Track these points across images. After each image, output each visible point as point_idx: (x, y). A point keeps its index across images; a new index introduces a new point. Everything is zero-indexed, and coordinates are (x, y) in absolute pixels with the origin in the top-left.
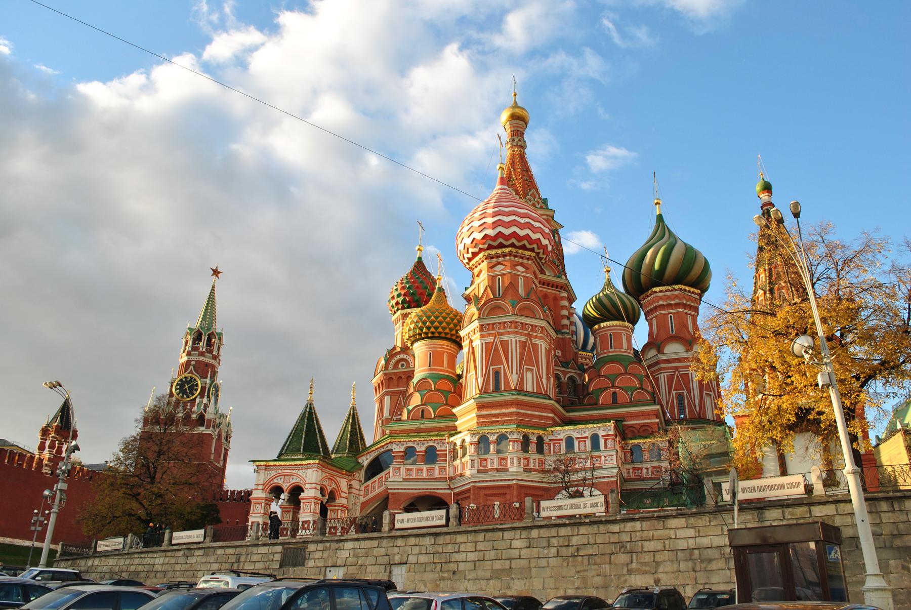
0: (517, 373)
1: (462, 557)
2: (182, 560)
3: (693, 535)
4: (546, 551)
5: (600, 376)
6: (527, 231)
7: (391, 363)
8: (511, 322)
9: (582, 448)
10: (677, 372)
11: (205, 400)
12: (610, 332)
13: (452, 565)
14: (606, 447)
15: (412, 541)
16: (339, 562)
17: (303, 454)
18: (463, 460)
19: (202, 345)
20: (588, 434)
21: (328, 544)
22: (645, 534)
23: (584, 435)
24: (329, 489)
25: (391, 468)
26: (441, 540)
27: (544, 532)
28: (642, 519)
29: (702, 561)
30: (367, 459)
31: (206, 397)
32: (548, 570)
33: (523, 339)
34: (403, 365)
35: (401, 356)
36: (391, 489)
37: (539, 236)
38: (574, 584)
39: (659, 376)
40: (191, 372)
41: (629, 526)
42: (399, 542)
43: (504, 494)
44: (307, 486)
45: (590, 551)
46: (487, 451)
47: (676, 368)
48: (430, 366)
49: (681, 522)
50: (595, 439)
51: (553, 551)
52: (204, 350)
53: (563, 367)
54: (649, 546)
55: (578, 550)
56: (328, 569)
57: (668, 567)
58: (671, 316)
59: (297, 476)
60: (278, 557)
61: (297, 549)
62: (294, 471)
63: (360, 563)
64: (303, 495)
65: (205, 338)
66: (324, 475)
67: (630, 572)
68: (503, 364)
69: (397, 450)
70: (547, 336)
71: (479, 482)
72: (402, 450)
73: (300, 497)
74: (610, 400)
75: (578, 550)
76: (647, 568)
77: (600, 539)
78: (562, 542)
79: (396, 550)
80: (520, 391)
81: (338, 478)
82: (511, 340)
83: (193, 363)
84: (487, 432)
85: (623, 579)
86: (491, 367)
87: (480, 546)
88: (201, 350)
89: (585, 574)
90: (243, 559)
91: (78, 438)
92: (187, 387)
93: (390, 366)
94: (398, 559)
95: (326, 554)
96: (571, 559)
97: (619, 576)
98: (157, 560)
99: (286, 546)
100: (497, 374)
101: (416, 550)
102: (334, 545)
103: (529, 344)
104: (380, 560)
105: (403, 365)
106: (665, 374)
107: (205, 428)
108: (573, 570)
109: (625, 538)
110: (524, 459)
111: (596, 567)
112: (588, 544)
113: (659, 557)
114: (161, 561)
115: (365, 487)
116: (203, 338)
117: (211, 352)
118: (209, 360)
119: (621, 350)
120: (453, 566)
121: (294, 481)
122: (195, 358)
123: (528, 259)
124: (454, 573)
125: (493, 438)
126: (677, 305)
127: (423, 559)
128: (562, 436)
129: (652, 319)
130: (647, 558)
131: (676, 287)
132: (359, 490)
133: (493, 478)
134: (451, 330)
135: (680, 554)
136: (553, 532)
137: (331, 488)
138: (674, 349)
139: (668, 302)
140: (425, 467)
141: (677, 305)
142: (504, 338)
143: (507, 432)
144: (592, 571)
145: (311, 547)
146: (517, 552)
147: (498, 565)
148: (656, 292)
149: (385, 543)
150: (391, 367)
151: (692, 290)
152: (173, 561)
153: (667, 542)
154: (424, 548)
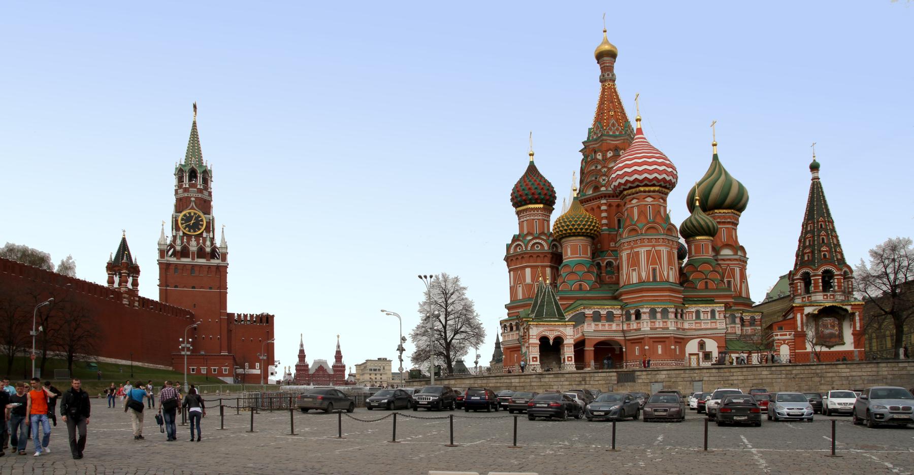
1: (736, 378)
2: (537, 380)
3: (849, 371)
4: (780, 376)
5: (698, 271)
6: (664, 176)
8: (663, 239)
9: (706, 317)
10: (728, 268)
12: (702, 243)
13: (730, 381)
14: (719, 317)
15: (705, 371)
16: (659, 380)
17: (558, 318)
20: (709, 310)
21: (650, 372)
22: (827, 370)
23: (707, 310)
25: (586, 323)
26: (722, 371)
27: (778, 368)
28: (826, 365)
29: (853, 381)
32: (782, 383)
35: (537, 241)
38: (794, 388)
40: (192, 208)
41: (820, 367)
42: (697, 371)
43: (664, 341)
44: (568, 337)
45: (802, 376)
46: (655, 317)
47: (728, 265)
48: (580, 255)
49: (844, 366)
50: (713, 312)
51: (784, 376)
54: (829, 375)
55: (796, 376)
56: (652, 384)
57: (838, 383)
59: (559, 331)
60: (615, 378)
61: (627, 374)
63: (673, 380)
67: (821, 384)
68: (658, 265)
69: (588, 313)
71: (650, 334)
72: (592, 313)
74: (703, 286)
75: (796, 376)
76: (829, 383)
77: (806, 372)
78: (788, 372)
79: (695, 375)
80: (667, 281)
85: (817, 387)
86: (651, 266)
87: (744, 373)
89: (799, 385)
90: (588, 379)
91: (140, 273)
92: (192, 222)
94: (697, 379)
95: (649, 377)
96: (793, 379)
97: (816, 386)
98: (513, 381)
99: (619, 373)
100: (654, 270)
101: (708, 375)
102: (656, 372)
104: (686, 379)
105: (537, 247)
108: (794, 384)
109: (818, 371)
111: (805, 382)
112: (801, 373)
113: (834, 379)
114: (517, 380)
120: (731, 382)
121: (556, 334)
124: (732, 384)
125: (658, 310)
126: (729, 223)
127: (712, 379)
128: (694, 310)
130: (828, 379)
131: (730, 211)
133: (660, 333)
135: (843, 378)
136: (783, 368)
138: (726, 252)
139: (723, 220)
140: (607, 324)
141: (729, 223)
142: (657, 248)
144: (803, 384)
145: (638, 373)
146: (765, 377)
147: (755, 381)
148: (717, 213)
149: (687, 371)
152: (529, 380)
153: (837, 374)
154: (712, 374)
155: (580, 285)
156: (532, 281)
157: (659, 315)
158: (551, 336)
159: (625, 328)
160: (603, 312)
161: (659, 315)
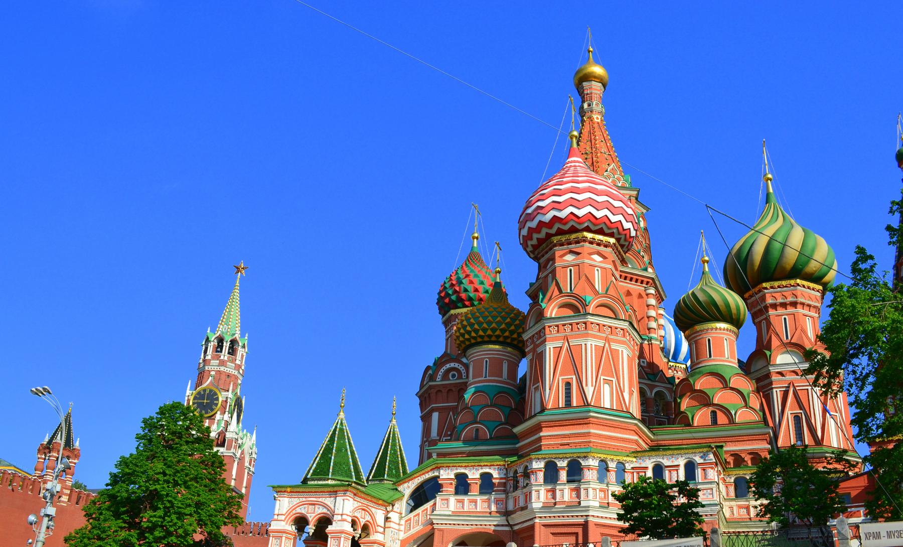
0: (592, 386)
7: (440, 373)
11: (226, 417)
18: (525, 490)
19: (224, 355)
24: (363, 522)
25: (438, 498)
30: (409, 487)
31: (227, 413)
33: (601, 343)
34: (454, 376)
36: (437, 524)
37: (620, 218)
39: (770, 392)
52: (226, 358)
53: (649, 379)
58: (785, 319)
59: (325, 506)
62: (320, 500)
64: (330, 528)
65: (226, 346)
66: (356, 504)
70: (629, 341)
73: (327, 530)
81: (373, 509)
82: (586, 344)
83: (213, 373)
84: (554, 456)
86: (561, 378)
88: (222, 358)
93: (439, 376)
100: (568, 385)
103: (607, 351)
106: (778, 390)
107: (225, 449)
110: (600, 491)
115: (406, 521)
116: (225, 344)
117: (234, 361)
118: (231, 370)
119: (723, 358)
121: (320, 510)
122: (215, 367)
123: (606, 246)
129: (760, 322)
132: (399, 524)
134: (512, 332)
137: (364, 521)
143: (579, 457)
148: (766, 288)
150: (439, 377)
151: (812, 285)
155: (477, 430)
156: (438, 435)
157: (563, 475)
158: (313, 515)
159: (511, 507)
160: (474, 474)
161: (563, 475)
